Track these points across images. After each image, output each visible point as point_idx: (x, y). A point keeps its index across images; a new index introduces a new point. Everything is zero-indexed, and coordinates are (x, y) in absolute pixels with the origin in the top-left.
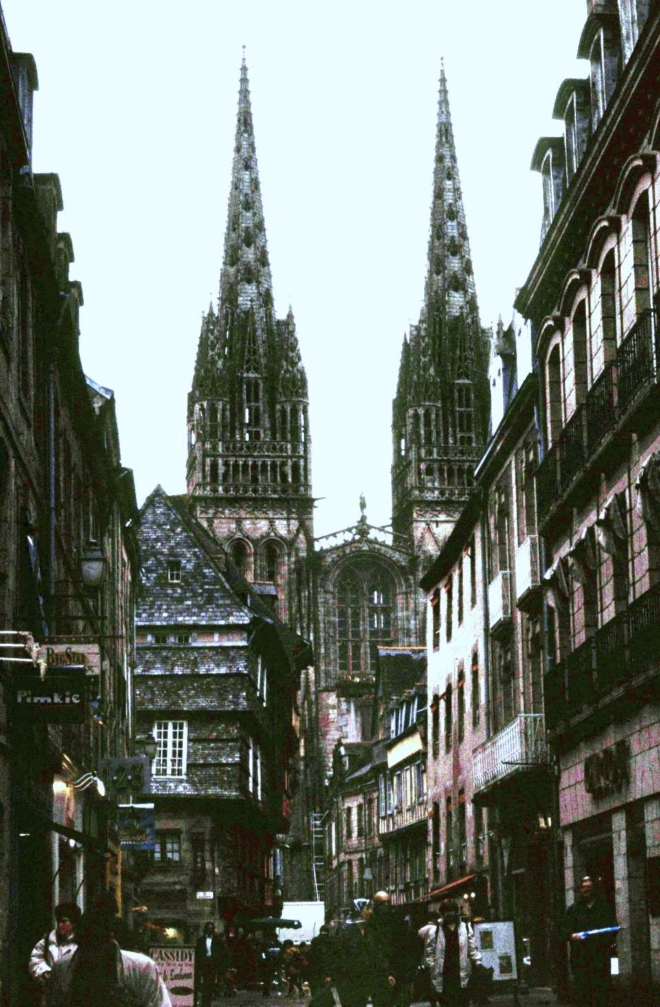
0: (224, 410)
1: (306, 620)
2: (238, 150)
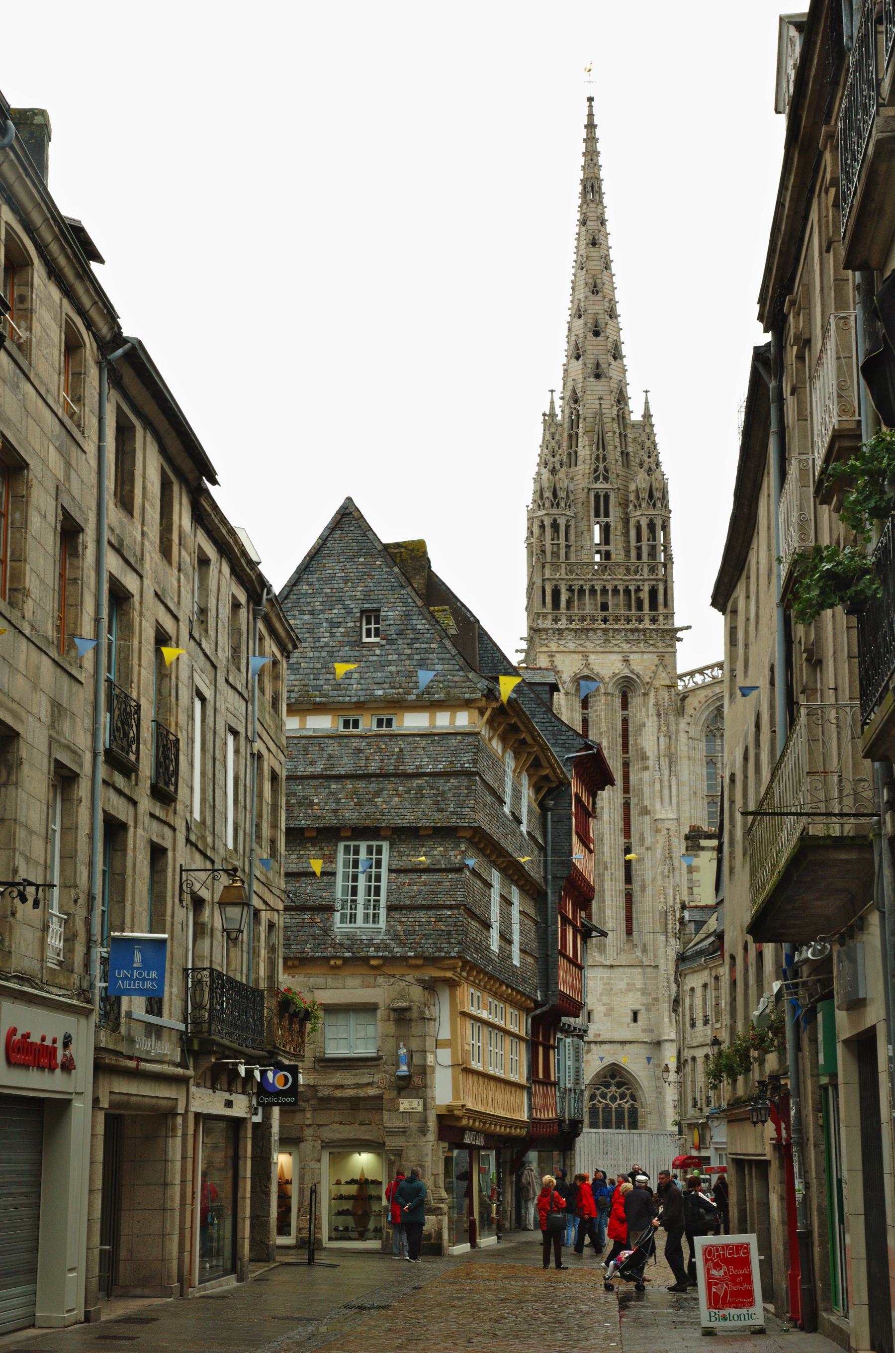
2: (583, 223)
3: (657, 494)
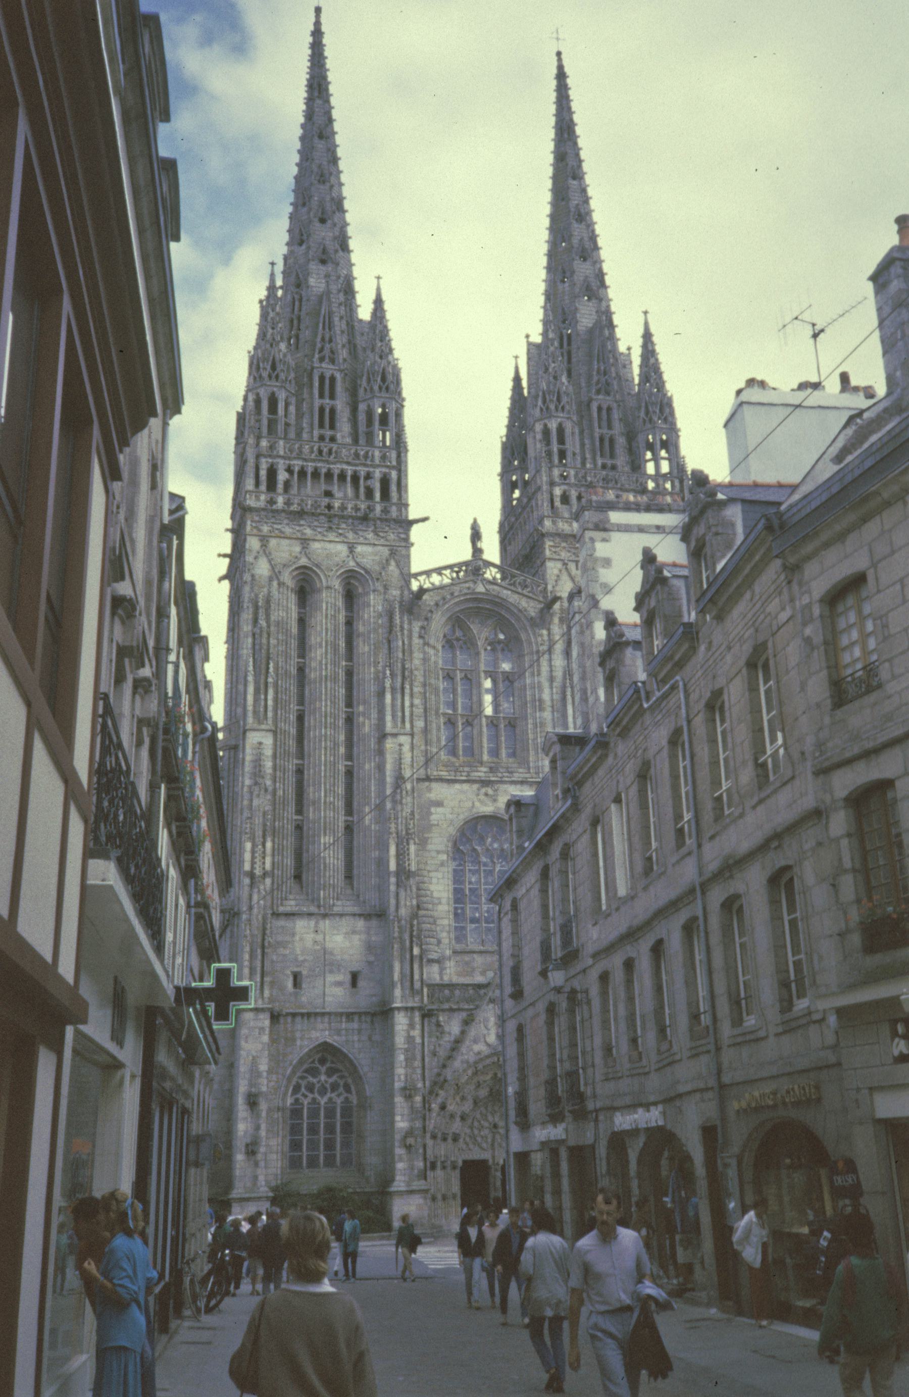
0: (287, 405)
1: (399, 679)
3: (390, 378)
